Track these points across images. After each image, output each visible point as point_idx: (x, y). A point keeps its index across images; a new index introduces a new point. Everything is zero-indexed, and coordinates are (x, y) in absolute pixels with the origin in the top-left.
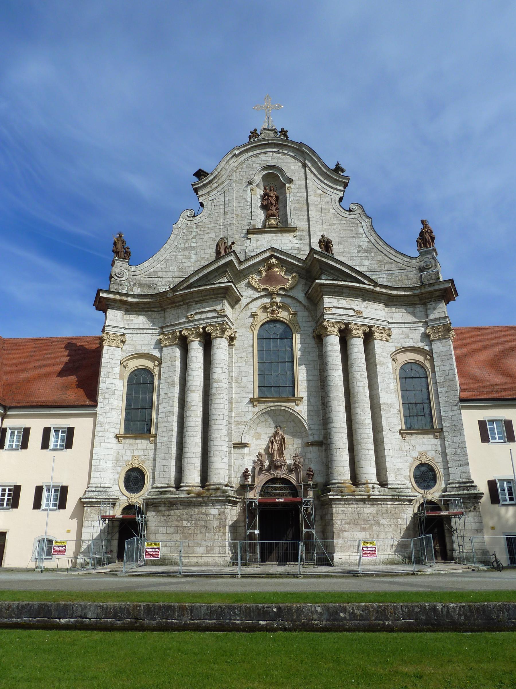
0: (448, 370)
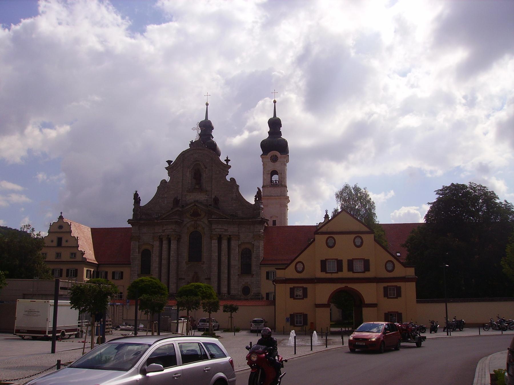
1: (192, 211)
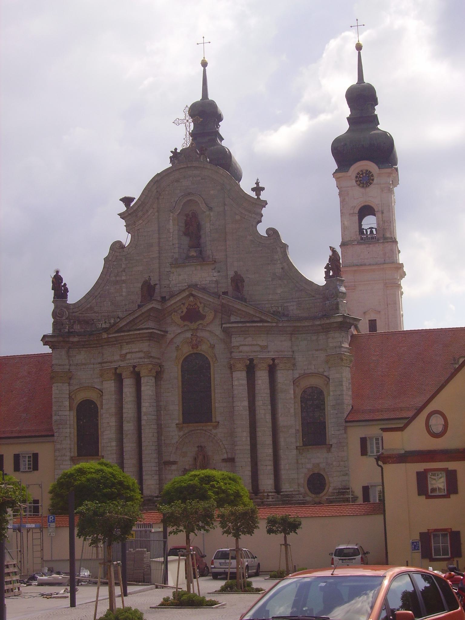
0: (339, 395)
1: (185, 310)
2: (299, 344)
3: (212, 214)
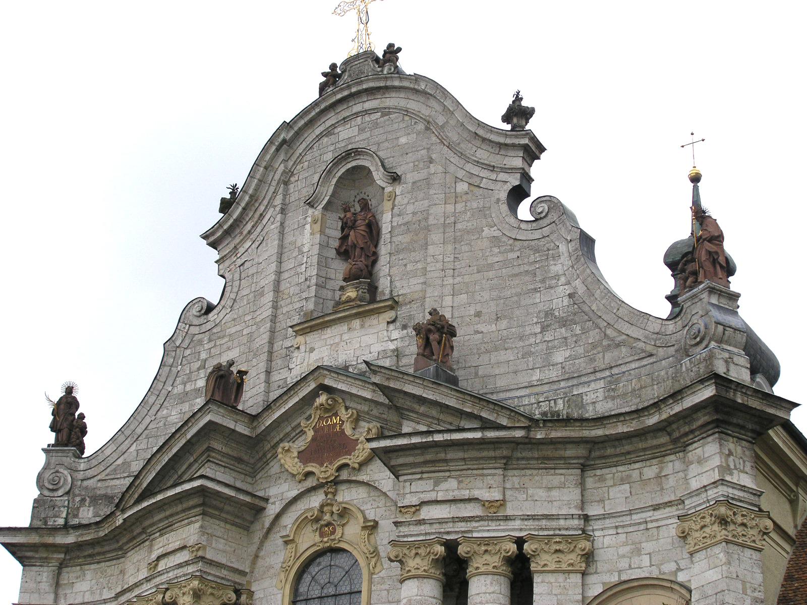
1: (310, 434)
2: (606, 495)
3: (399, 189)
